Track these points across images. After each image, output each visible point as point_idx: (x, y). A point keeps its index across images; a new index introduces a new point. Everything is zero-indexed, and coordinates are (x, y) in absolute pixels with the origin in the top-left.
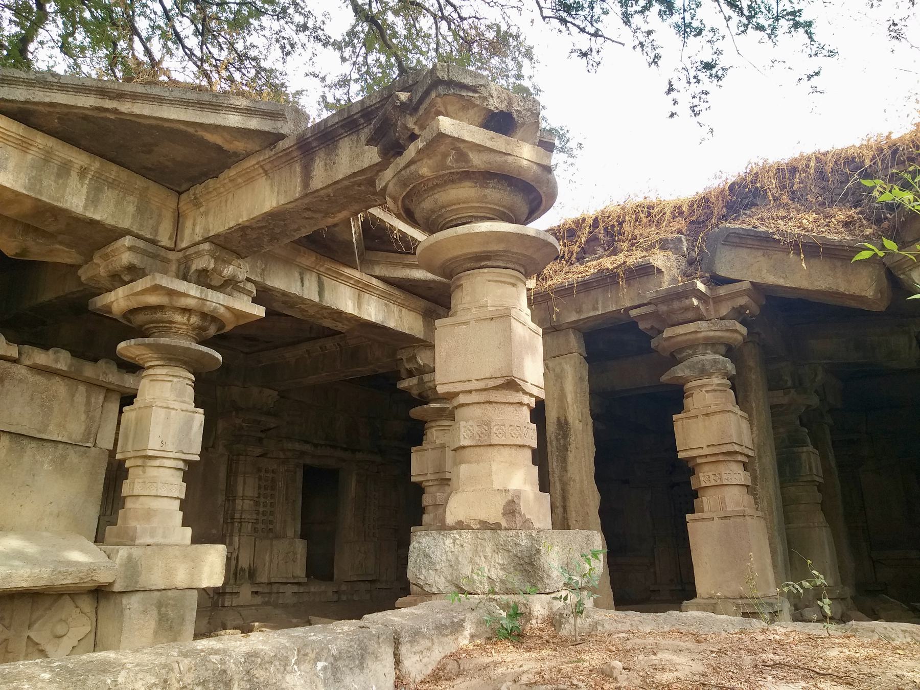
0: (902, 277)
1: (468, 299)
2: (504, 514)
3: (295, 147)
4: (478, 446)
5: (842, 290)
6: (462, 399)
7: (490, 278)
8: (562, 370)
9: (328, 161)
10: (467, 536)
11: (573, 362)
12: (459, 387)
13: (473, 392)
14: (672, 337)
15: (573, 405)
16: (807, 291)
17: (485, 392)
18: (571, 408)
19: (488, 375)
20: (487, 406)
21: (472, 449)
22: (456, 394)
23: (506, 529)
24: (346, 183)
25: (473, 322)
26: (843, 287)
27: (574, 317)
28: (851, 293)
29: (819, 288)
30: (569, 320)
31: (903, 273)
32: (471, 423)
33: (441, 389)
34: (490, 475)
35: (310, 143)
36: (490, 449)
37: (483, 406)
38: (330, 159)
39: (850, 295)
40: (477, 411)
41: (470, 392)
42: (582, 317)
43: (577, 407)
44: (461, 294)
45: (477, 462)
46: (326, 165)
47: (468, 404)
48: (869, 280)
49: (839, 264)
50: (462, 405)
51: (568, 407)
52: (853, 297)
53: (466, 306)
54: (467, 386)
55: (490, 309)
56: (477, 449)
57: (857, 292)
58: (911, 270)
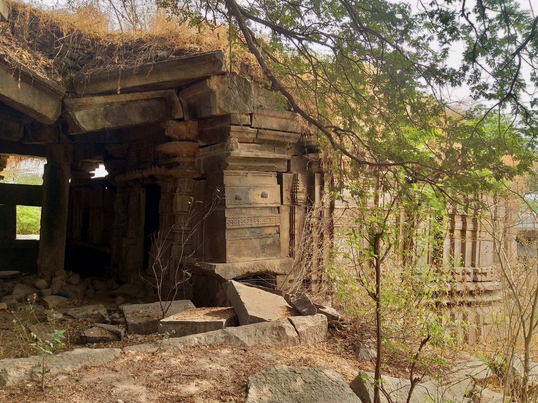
0: (70, 113)
5: (35, 109)
16: (14, 101)
26: (36, 107)
28: (40, 112)
29: (22, 103)
31: (71, 111)
39: (39, 113)
48: (52, 109)
49: (37, 92)
52: (40, 115)
57: (44, 113)
58: (76, 111)
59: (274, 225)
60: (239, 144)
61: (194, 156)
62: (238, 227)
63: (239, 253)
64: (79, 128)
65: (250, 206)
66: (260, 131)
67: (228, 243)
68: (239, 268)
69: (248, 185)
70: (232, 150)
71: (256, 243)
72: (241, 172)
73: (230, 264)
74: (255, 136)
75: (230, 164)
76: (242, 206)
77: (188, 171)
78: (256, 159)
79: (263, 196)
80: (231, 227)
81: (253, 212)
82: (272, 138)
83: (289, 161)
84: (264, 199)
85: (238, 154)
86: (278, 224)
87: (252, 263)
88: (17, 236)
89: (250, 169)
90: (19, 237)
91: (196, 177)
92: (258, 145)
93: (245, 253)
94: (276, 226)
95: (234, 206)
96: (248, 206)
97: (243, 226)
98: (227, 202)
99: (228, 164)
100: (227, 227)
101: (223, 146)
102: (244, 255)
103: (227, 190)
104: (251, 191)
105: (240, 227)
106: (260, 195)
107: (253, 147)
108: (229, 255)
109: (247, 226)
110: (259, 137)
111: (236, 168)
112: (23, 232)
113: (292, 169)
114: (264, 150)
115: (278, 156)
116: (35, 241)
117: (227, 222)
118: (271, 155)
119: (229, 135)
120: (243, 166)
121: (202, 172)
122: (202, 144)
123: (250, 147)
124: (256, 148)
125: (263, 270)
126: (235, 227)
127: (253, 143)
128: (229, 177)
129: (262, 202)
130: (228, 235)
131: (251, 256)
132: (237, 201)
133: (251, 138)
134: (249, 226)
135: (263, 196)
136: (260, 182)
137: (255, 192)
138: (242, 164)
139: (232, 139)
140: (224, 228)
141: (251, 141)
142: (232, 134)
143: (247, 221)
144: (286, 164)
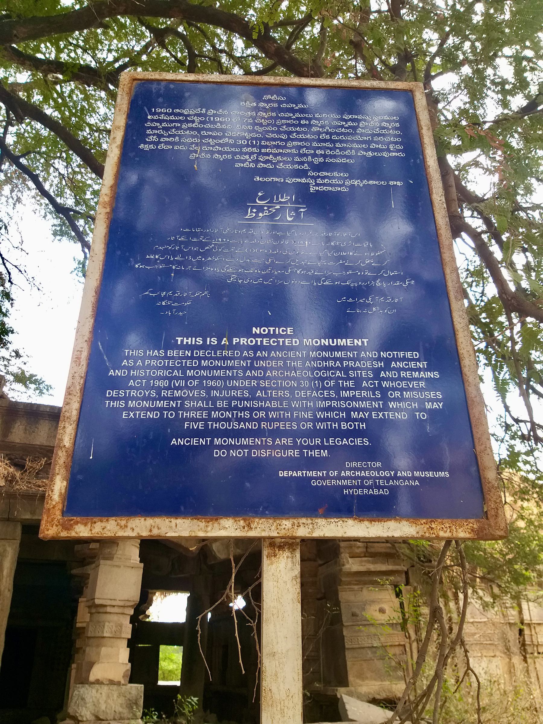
1: (120, 552)
2: (123, 677)
3: (5, 408)
4: (113, 638)
5: (183, 544)
6: (109, 609)
7: (133, 544)
8: (5, 550)
9: (28, 428)
10: (105, 689)
11: (14, 547)
12: (109, 603)
13: (116, 607)
14: (94, 549)
15: (6, 578)
17: (122, 608)
18: (4, 580)
19: (126, 599)
20: (121, 616)
21: (108, 639)
22: (105, 606)
23: (123, 685)
24: (37, 447)
25: (122, 566)
27: (28, 516)
30: (24, 517)
32: (111, 624)
33: (97, 602)
34: (118, 655)
35: (19, 411)
36: (118, 640)
37: (119, 615)
38: (30, 427)
40: (115, 618)
41: (114, 606)
42: (34, 518)
43: (10, 580)
44: (116, 548)
45: (112, 647)
46: (26, 429)
47: (110, 613)
50: (106, 613)
51: (3, 578)
53: (119, 556)
54: (114, 603)
55: (132, 561)
56: (112, 640)
59: (397, 643)
60: (349, 559)
61: (316, 575)
62: (357, 646)
63: (361, 676)
64: (215, 557)
65: (369, 623)
66: (369, 544)
67: (349, 664)
68: (363, 693)
69: (364, 600)
70: (343, 565)
71: (379, 664)
72: (356, 587)
73: (353, 689)
74: (365, 550)
75: (343, 579)
76: (360, 623)
77: (310, 591)
78: (369, 573)
79: (382, 611)
80: (351, 647)
81: (373, 630)
82: (383, 550)
83: (407, 573)
84: (381, 614)
85: (350, 569)
86: (402, 643)
87: (377, 687)
88: (159, 682)
89: (365, 583)
90: (161, 683)
91: (319, 596)
92: (370, 559)
93: (368, 676)
94: (399, 645)
95: (351, 623)
96: (366, 623)
97: (363, 646)
98: (344, 618)
99: (341, 580)
100: (347, 646)
101: (336, 563)
102: (367, 678)
103: (343, 606)
104: (367, 607)
105: (360, 646)
106: (378, 610)
107: (365, 561)
108: (351, 678)
109: (367, 645)
110: (369, 550)
111: (349, 583)
112: (164, 679)
113: (411, 580)
114: (376, 563)
115: (390, 567)
116: (176, 686)
117: (346, 641)
118: (384, 567)
119: (340, 551)
120: (356, 581)
121: (323, 591)
122: (321, 562)
123: (361, 561)
124: (369, 562)
125: (390, 696)
126: (355, 646)
127: (365, 556)
128: (344, 593)
129: (382, 618)
130: (349, 655)
131: (375, 680)
132: (354, 618)
133: (361, 552)
134: (370, 645)
135: (382, 611)
136: (377, 597)
137: (372, 608)
138: (358, 579)
139: (343, 555)
140: (343, 648)
141: (362, 555)
142: (342, 550)
143: (366, 639)
144: (404, 576)
